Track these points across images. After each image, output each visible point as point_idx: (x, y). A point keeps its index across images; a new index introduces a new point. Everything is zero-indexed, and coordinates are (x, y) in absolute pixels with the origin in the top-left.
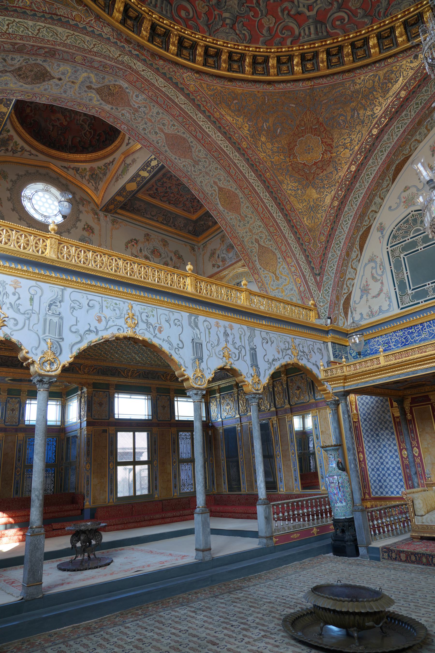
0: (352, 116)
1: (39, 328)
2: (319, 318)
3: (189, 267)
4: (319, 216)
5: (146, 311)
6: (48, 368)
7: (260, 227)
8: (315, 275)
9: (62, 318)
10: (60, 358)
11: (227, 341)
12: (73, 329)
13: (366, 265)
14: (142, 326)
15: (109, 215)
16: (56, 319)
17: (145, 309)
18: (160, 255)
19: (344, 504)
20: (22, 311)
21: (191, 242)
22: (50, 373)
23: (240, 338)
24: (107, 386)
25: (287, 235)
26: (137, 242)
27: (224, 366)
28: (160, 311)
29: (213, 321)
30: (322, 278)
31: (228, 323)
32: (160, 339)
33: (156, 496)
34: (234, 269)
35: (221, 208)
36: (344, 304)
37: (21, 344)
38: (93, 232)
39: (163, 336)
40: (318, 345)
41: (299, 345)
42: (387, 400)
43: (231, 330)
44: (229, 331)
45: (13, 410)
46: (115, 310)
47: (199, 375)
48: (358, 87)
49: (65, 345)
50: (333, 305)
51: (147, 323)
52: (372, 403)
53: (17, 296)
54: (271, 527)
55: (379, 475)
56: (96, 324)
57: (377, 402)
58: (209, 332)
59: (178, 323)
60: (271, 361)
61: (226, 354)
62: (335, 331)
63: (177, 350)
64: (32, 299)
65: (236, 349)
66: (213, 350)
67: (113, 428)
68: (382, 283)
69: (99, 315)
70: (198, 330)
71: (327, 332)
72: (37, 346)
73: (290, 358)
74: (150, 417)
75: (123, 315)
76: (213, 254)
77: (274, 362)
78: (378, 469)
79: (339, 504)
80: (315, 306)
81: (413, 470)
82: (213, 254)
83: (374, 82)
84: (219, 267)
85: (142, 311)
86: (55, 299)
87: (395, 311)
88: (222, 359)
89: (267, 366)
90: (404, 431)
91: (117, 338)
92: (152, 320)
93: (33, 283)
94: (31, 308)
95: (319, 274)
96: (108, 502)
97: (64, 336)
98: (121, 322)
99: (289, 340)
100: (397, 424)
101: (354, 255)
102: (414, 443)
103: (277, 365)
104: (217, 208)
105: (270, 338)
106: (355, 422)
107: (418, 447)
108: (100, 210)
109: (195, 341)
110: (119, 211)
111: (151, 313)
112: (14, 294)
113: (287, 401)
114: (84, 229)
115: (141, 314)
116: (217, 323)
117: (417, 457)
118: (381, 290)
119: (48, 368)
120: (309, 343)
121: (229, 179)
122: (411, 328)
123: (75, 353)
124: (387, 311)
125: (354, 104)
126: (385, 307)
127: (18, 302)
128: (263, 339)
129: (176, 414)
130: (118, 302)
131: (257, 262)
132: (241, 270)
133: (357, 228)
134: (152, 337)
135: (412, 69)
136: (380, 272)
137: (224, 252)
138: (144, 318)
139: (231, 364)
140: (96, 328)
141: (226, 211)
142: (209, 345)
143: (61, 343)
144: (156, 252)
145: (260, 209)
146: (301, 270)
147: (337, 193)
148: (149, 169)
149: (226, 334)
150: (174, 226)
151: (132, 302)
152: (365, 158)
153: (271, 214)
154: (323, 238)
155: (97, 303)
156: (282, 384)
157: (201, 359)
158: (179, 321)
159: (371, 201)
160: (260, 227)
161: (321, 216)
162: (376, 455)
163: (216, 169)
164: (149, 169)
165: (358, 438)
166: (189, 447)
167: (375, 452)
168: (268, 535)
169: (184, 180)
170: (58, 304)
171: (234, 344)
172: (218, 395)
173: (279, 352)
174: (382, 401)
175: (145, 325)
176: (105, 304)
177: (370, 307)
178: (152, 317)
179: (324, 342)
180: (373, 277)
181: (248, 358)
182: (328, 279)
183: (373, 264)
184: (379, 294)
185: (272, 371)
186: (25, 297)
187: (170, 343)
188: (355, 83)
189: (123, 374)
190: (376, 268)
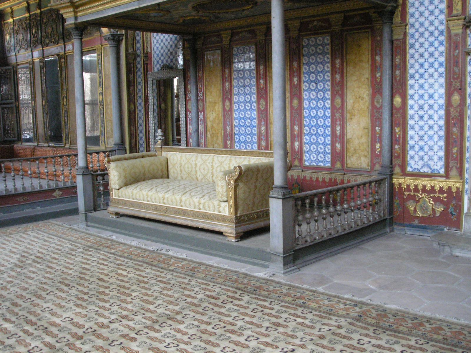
42: (180, 39)
52: (167, 40)
57: (171, 39)
102: (200, 95)
117: (201, 112)
174: (176, 38)
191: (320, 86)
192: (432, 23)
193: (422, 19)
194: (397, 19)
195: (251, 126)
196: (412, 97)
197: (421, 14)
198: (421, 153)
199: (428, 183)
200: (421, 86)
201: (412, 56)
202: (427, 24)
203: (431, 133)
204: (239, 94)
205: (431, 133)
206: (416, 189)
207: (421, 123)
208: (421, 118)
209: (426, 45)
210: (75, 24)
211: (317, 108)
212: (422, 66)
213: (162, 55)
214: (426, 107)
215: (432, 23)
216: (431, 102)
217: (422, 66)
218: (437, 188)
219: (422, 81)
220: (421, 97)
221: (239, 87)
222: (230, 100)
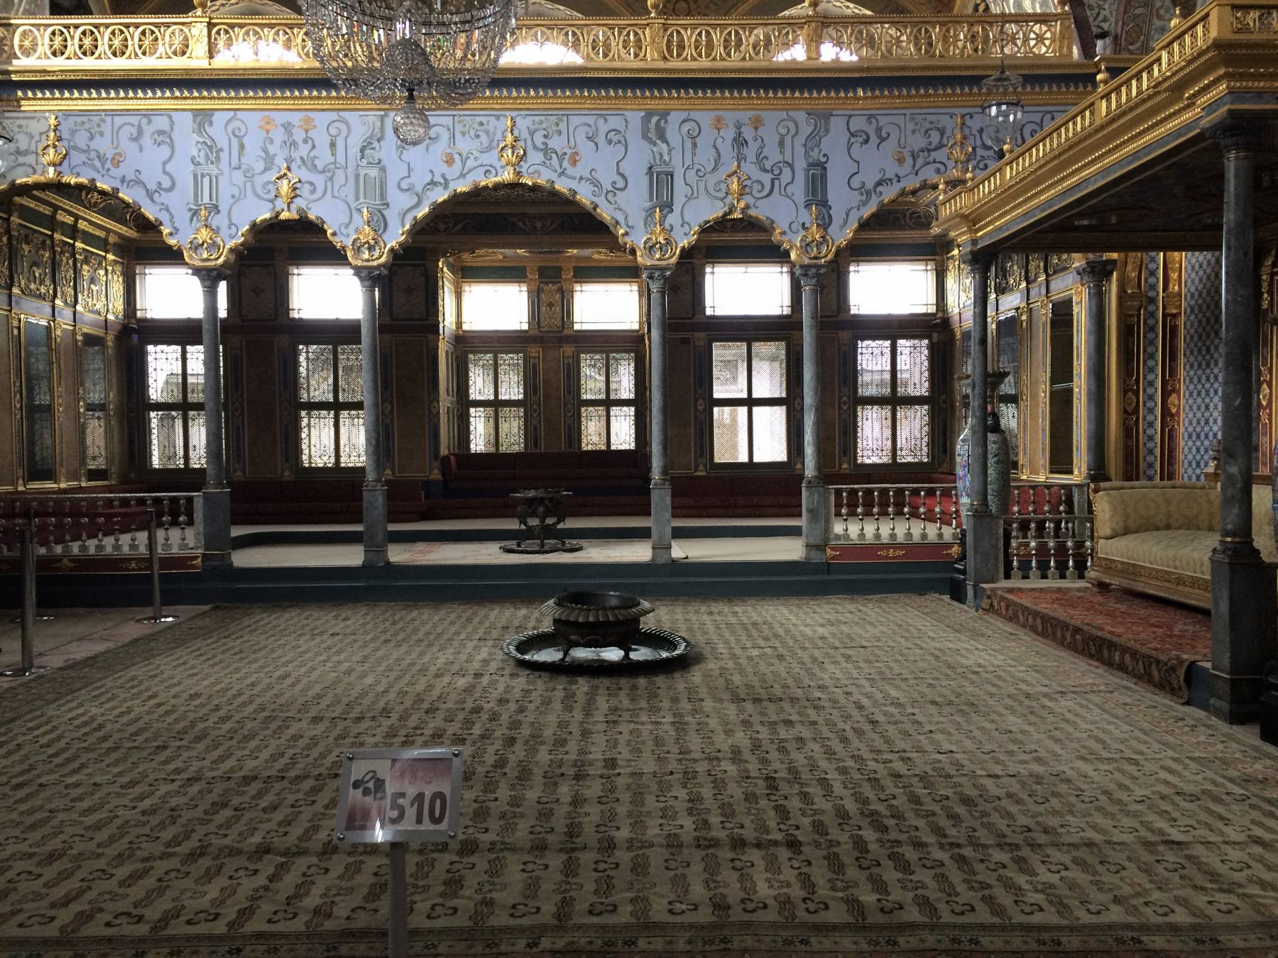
1: (349, 191)
5: (544, 126)
6: (366, 256)
9: (383, 169)
10: (385, 237)
11: (740, 158)
12: (404, 185)
14: (535, 157)
16: (373, 173)
17: (541, 122)
20: (320, 167)
22: (371, 264)
23: (781, 144)
27: (726, 214)
28: (575, 120)
29: (706, 118)
31: (750, 114)
32: (574, 178)
37: (323, 222)
39: (582, 169)
41: (981, 131)
43: (756, 129)
44: (748, 133)
45: (550, 305)
46: (478, 136)
47: (661, 239)
49: (392, 215)
51: (546, 151)
53: (309, 145)
54: (827, 529)
55: (1198, 450)
56: (444, 169)
58: (695, 145)
59: (618, 139)
60: (870, 185)
61: (735, 186)
63: (610, 195)
64: (333, 145)
65: (767, 171)
66: (702, 185)
67: (702, 335)
69: (449, 151)
70: (664, 146)
72: (347, 221)
73: (938, 171)
75: (495, 143)
77: (880, 189)
78: (1198, 436)
85: (536, 126)
86: (370, 137)
88: (722, 199)
89: (856, 198)
92: (556, 143)
93: (334, 116)
94: (332, 159)
97: (389, 200)
105: (879, 130)
106: (1174, 316)
109: (656, 169)
111: (554, 128)
112: (305, 141)
113: (1042, 265)
115: (532, 134)
116: (718, 120)
119: (366, 256)
123: (407, 227)
127: (312, 154)
128: (853, 135)
130: (484, 120)
134: (554, 177)
138: (539, 139)
139: (748, 207)
140: (443, 176)
142: (691, 173)
143: (385, 212)
149: (740, 142)
151: (514, 114)
155: (445, 130)
157: (667, 207)
158: (618, 132)
162: (1199, 401)
165: (1173, 357)
167: (1199, 394)
168: (818, 542)
170: (376, 144)
171: (760, 159)
173: (901, 161)
175: (541, 155)
176: (459, 128)
178: (556, 136)
181: (799, 190)
185: (867, 212)
186: (322, 140)
187: (596, 183)
210: (971, 252)
213: (1200, 295)
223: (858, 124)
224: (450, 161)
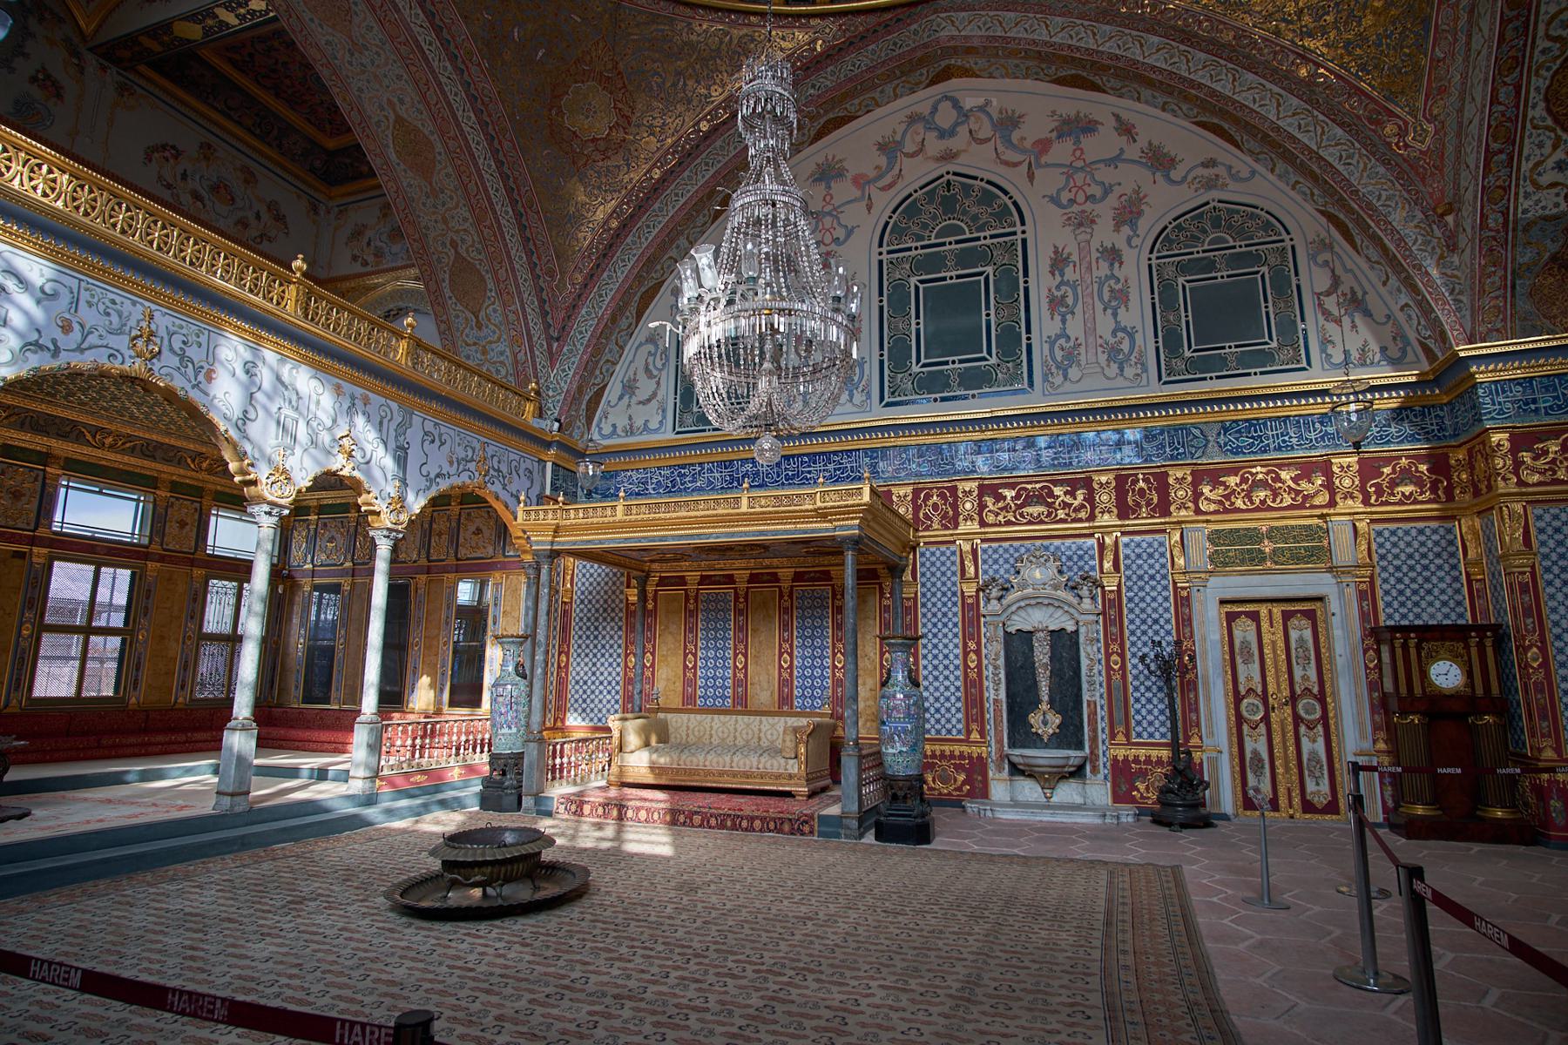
0: (674, 85)
2: (540, 416)
3: (298, 263)
4: (581, 235)
5: (184, 331)
7: (465, 220)
8: (550, 339)
13: (641, 345)
15: (114, 69)
18: (233, 199)
19: (514, 730)
21: (311, 192)
24: (45, 458)
25: (513, 252)
26: (178, 154)
30: (561, 348)
31: (362, 391)
33: (133, 700)
34: (397, 279)
35: (393, 157)
36: (589, 401)
38: (59, 96)
40: (528, 464)
46: (108, 314)
48: (694, 38)
50: (574, 399)
51: (183, 357)
56: (57, 334)
60: (432, 476)
62: (562, 446)
67: (45, 551)
68: (658, 383)
71: (548, 445)
74: (146, 541)
76: (357, 233)
79: (505, 730)
80: (538, 393)
81: (638, 686)
82: (357, 233)
83: (721, 43)
84: (365, 264)
87: (667, 436)
90: (638, 627)
91: (105, 374)
95: (558, 339)
96: (6, 707)
98: (121, 343)
99: (478, 446)
100: (630, 614)
101: (624, 323)
103: (444, 485)
104: (384, 152)
105: (440, 435)
107: (653, 654)
108: (90, 50)
110: (142, 68)
113: (452, 552)
114: (34, 79)
115: (171, 335)
118: (654, 395)
120: (512, 457)
121: (421, 107)
122: (683, 466)
124: (656, 431)
125: (682, 64)
126: (653, 425)
128: (426, 434)
129: (210, 542)
130: (118, 299)
131: (446, 284)
132: (411, 284)
133: (639, 278)
135: (782, 49)
136: (659, 364)
137: (384, 237)
138: (177, 345)
140: (54, 341)
141: (403, 166)
144: (223, 191)
145: (471, 186)
146: (527, 324)
147: (619, 206)
148: (242, 11)
150: (280, 146)
151: (154, 307)
152: (680, 164)
153: (491, 204)
154: (579, 278)
155: (66, 291)
156: (449, 520)
159: (672, 241)
160: (465, 220)
161: (586, 237)
163: (399, 77)
164: (242, 11)
165: (565, 629)
166: (229, 612)
169: (325, 73)
172: (313, 517)
173: (451, 463)
176: (85, 295)
177: (630, 418)
179: (540, 460)
180: (647, 370)
182: (570, 351)
183: (651, 348)
184: (649, 400)
188: (691, 31)
189: (89, 437)
190: (655, 355)
191: (818, 642)
192: (944, 584)
193: (933, 579)
194: (908, 576)
195: (724, 687)
196: (925, 657)
197: (933, 574)
198: (938, 716)
199: (947, 748)
200: (935, 646)
201: (924, 615)
202: (939, 584)
203: (947, 694)
204: (707, 648)
205: (947, 694)
206: (934, 756)
207: (936, 684)
208: (936, 678)
209: (939, 605)
211: (813, 667)
212: (935, 625)
214: (941, 668)
215: (944, 584)
216: (946, 662)
217: (935, 625)
218: (957, 753)
219: (935, 641)
220: (935, 657)
221: (707, 639)
222: (695, 655)
223: (429, 426)
224: (66, 328)
